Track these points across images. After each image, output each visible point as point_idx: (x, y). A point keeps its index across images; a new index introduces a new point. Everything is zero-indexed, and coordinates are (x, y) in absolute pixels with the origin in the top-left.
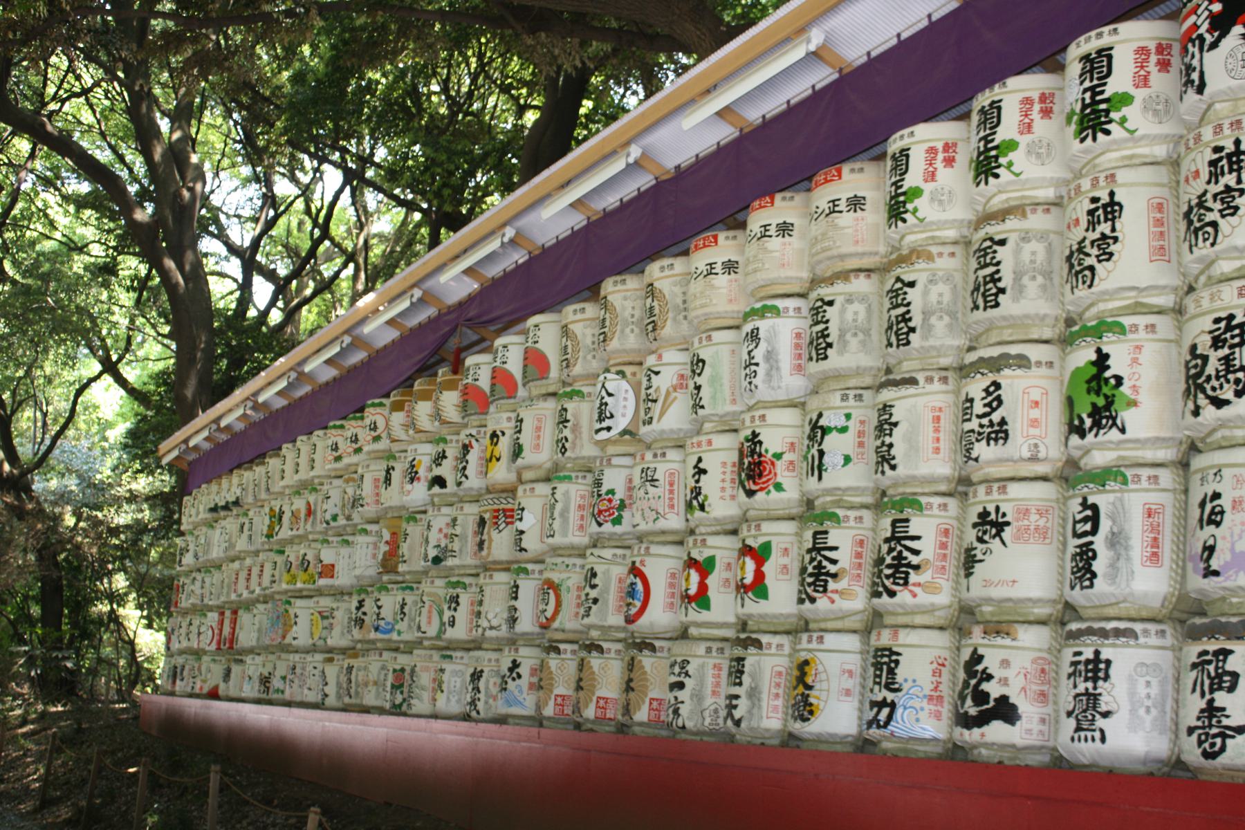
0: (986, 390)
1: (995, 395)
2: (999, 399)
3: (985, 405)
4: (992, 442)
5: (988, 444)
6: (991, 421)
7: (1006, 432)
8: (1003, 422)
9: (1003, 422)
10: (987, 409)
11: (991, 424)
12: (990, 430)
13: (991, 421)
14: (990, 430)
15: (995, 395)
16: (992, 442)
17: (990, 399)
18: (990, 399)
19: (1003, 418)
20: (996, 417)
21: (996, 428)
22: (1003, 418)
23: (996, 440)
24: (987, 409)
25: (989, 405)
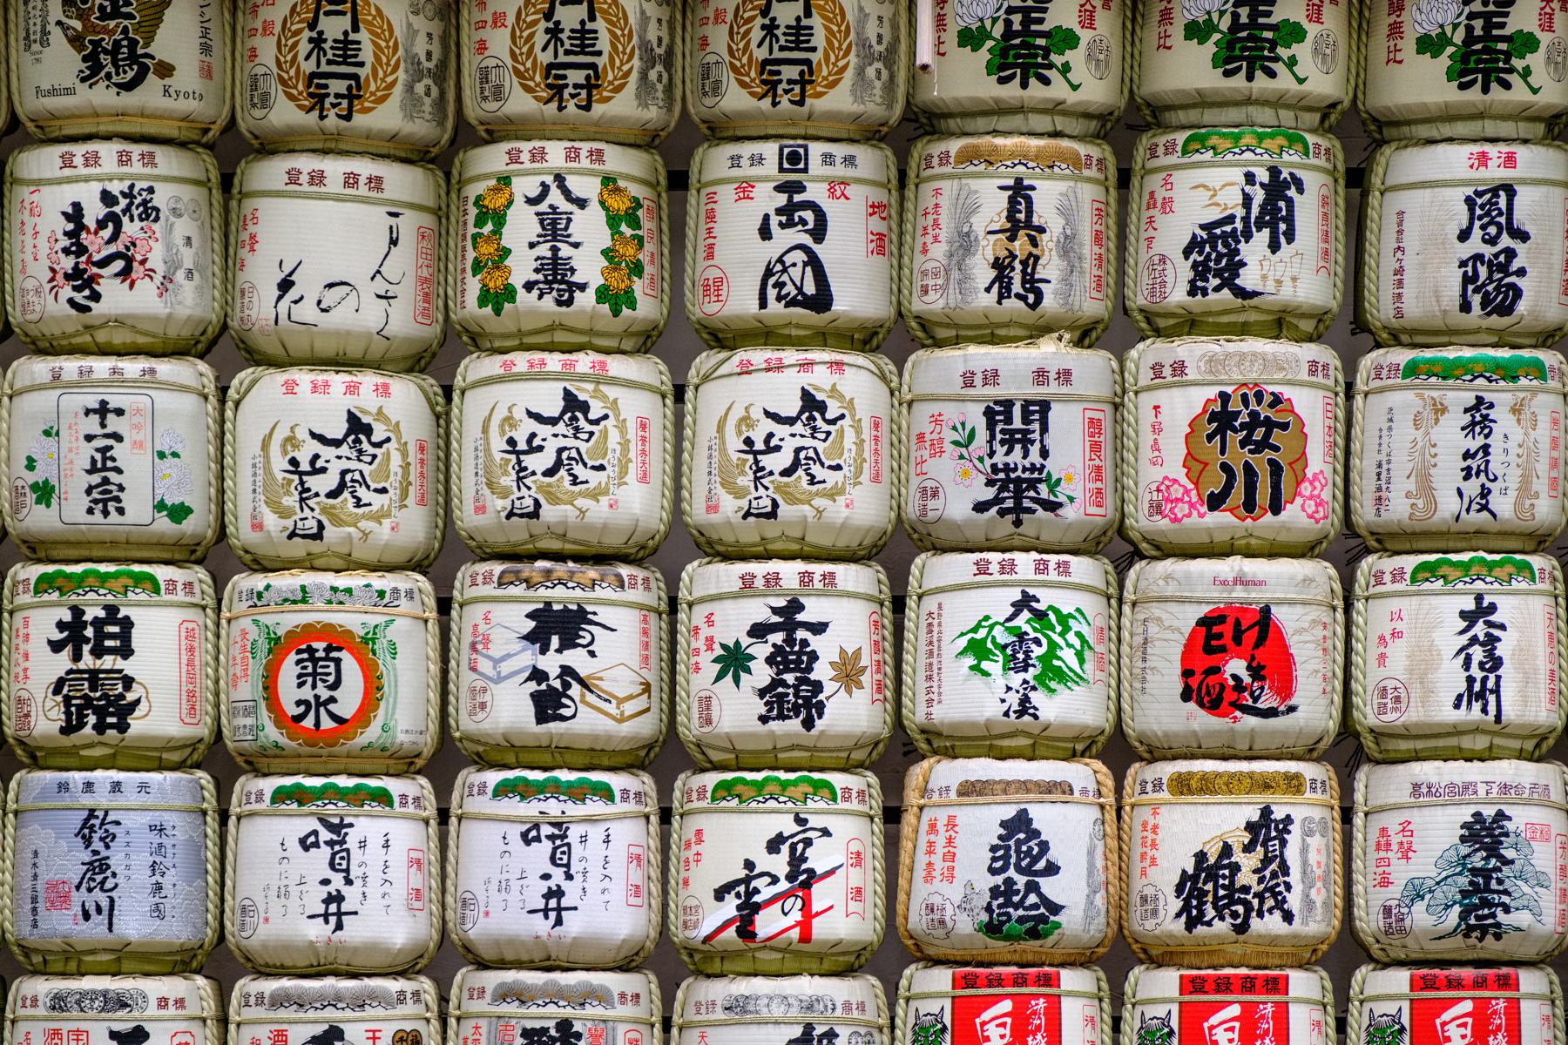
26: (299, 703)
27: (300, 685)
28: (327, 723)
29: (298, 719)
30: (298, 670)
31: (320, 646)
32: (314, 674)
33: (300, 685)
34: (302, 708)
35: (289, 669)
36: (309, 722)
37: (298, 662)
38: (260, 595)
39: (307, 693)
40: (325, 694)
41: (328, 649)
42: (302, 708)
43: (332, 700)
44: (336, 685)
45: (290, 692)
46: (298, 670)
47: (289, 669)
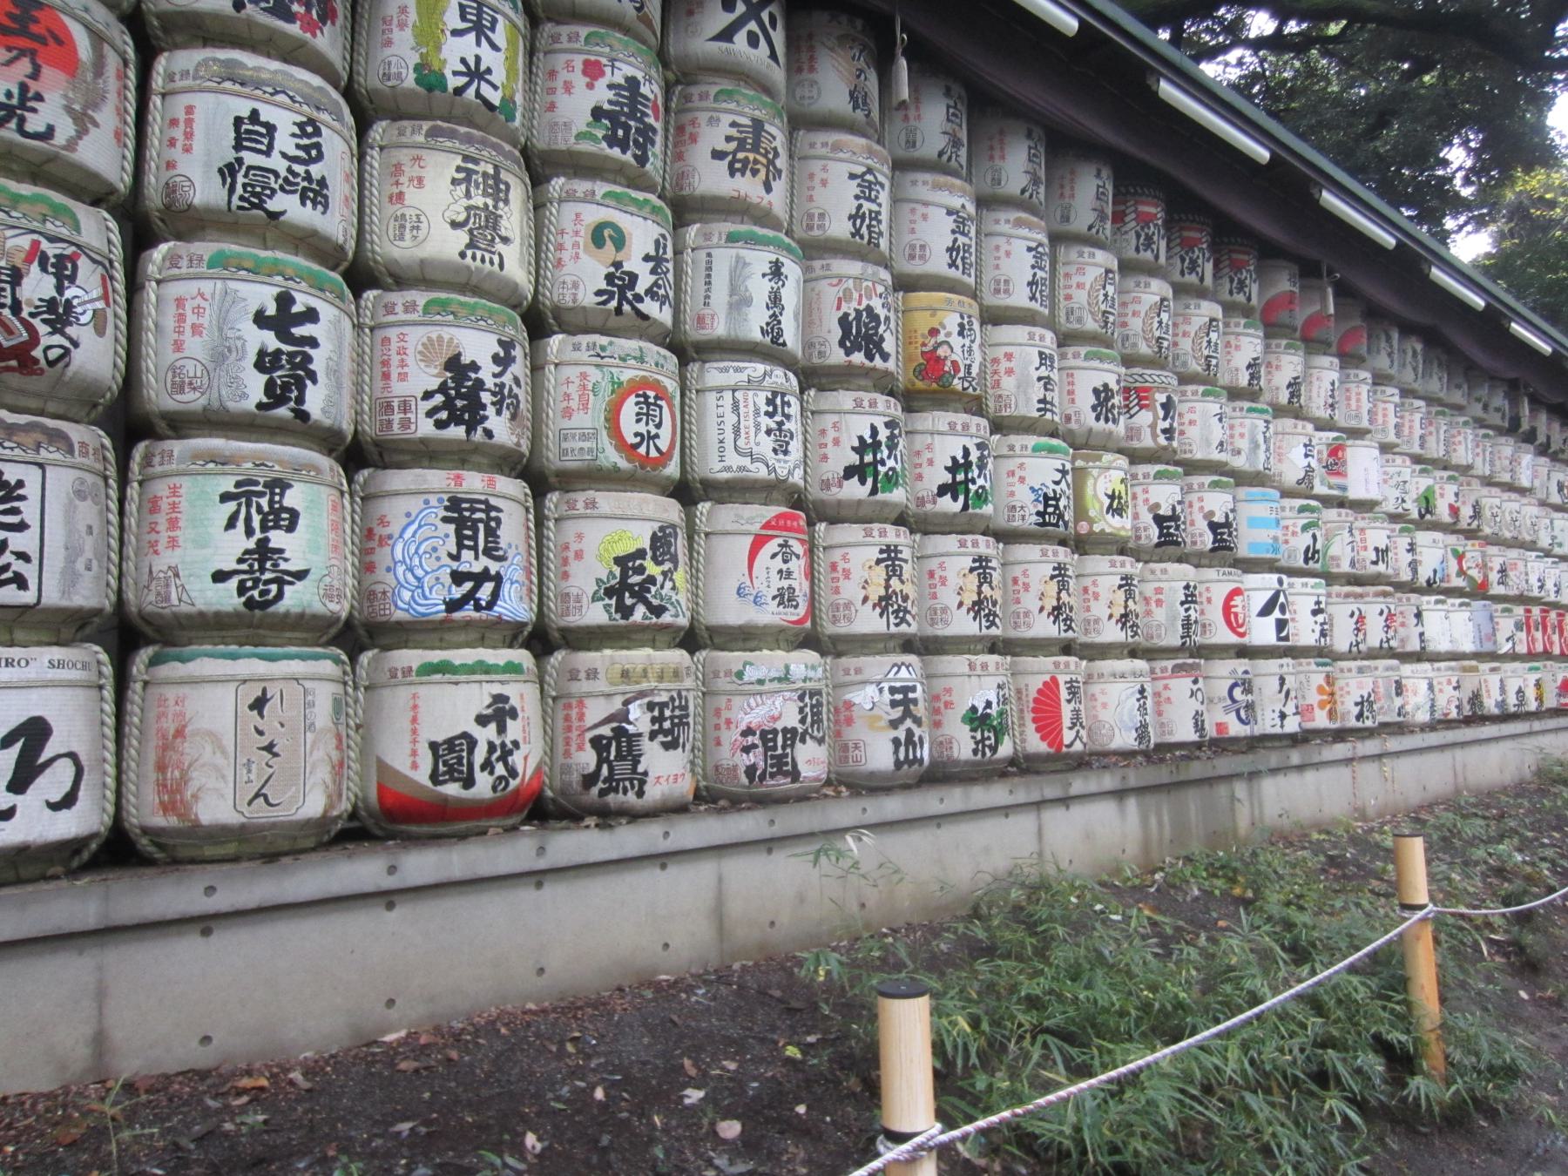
0: (301, 126)
1: (315, 140)
2: (318, 146)
3: (298, 146)
4: (309, 203)
5: (303, 204)
6: (307, 172)
7: (326, 197)
8: (322, 182)
9: (322, 182)
10: (301, 154)
11: (308, 177)
12: (306, 184)
13: (307, 172)
14: (306, 184)
15: (315, 140)
16: (309, 203)
17: (305, 141)
18: (305, 141)
19: (323, 178)
20: (316, 170)
21: (314, 186)
22: (323, 178)
23: (315, 203)
24: (301, 154)
25: (306, 148)
26: (636, 435)
27: (638, 421)
28: (653, 453)
29: (636, 446)
30: (636, 409)
31: (651, 394)
32: (647, 415)
33: (638, 421)
34: (638, 439)
35: (630, 408)
36: (642, 450)
37: (637, 403)
38: (603, 348)
39: (642, 428)
40: (654, 431)
41: (656, 398)
42: (638, 439)
43: (657, 436)
44: (658, 426)
45: (630, 426)
46: (636, 409)
47: (630, 408)
